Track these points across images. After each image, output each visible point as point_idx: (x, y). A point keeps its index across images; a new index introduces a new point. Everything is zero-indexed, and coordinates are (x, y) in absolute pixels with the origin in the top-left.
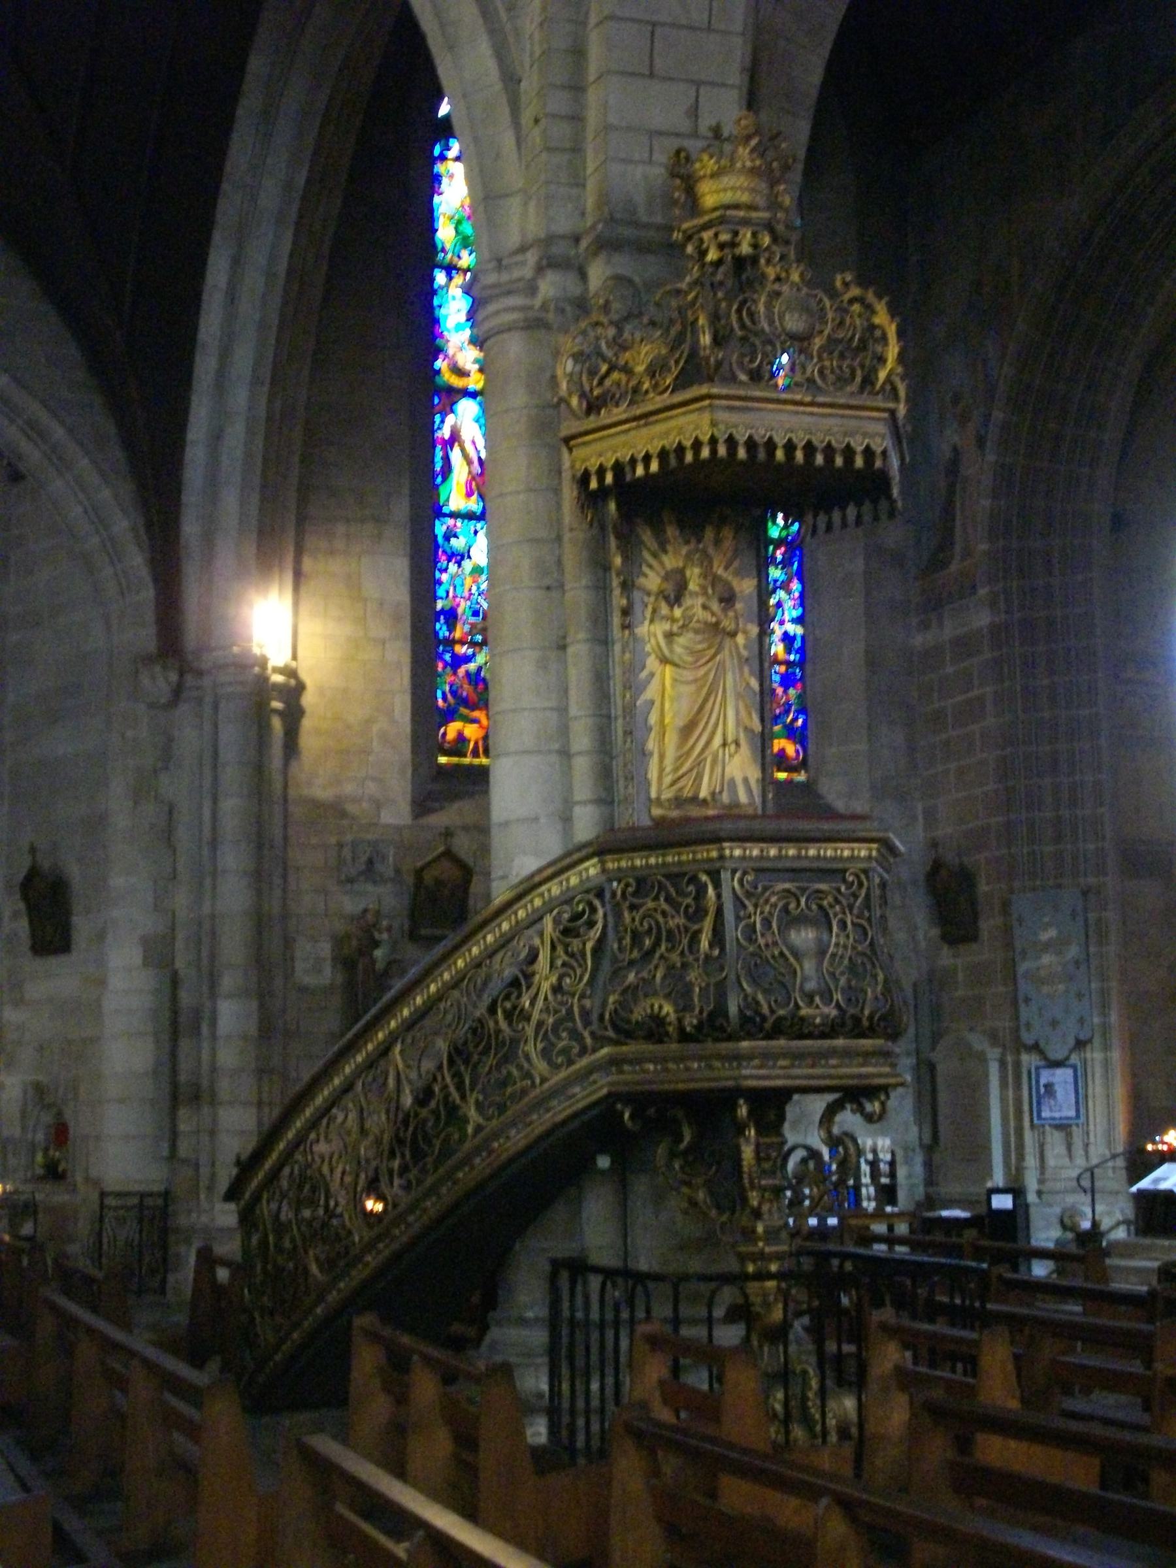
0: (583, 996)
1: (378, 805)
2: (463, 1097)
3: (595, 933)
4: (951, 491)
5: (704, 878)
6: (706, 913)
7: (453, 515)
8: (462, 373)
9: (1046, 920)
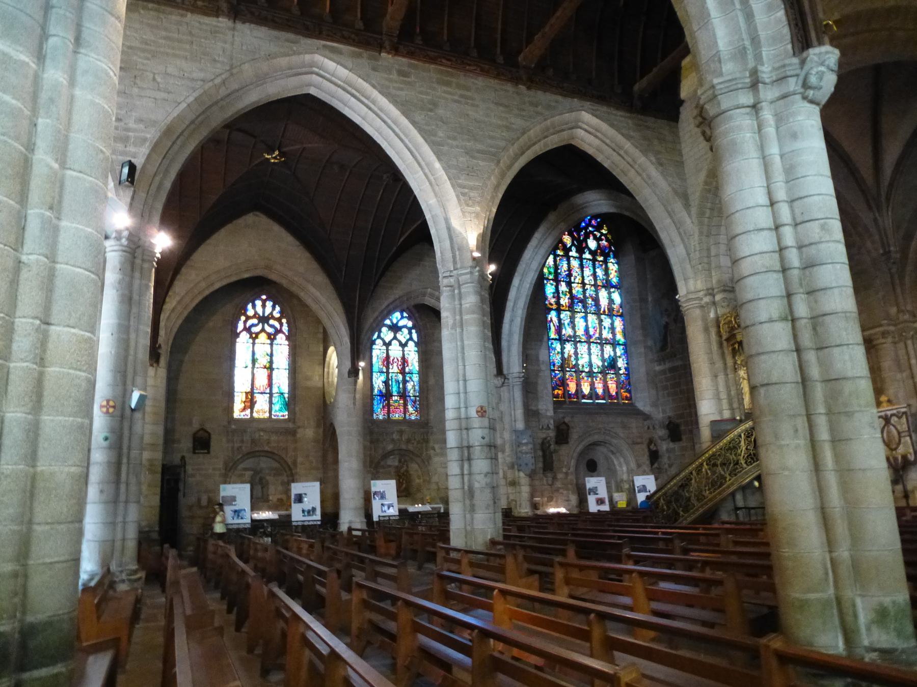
1: (546, 410)
7: (553, 339)
8: (551, 304)
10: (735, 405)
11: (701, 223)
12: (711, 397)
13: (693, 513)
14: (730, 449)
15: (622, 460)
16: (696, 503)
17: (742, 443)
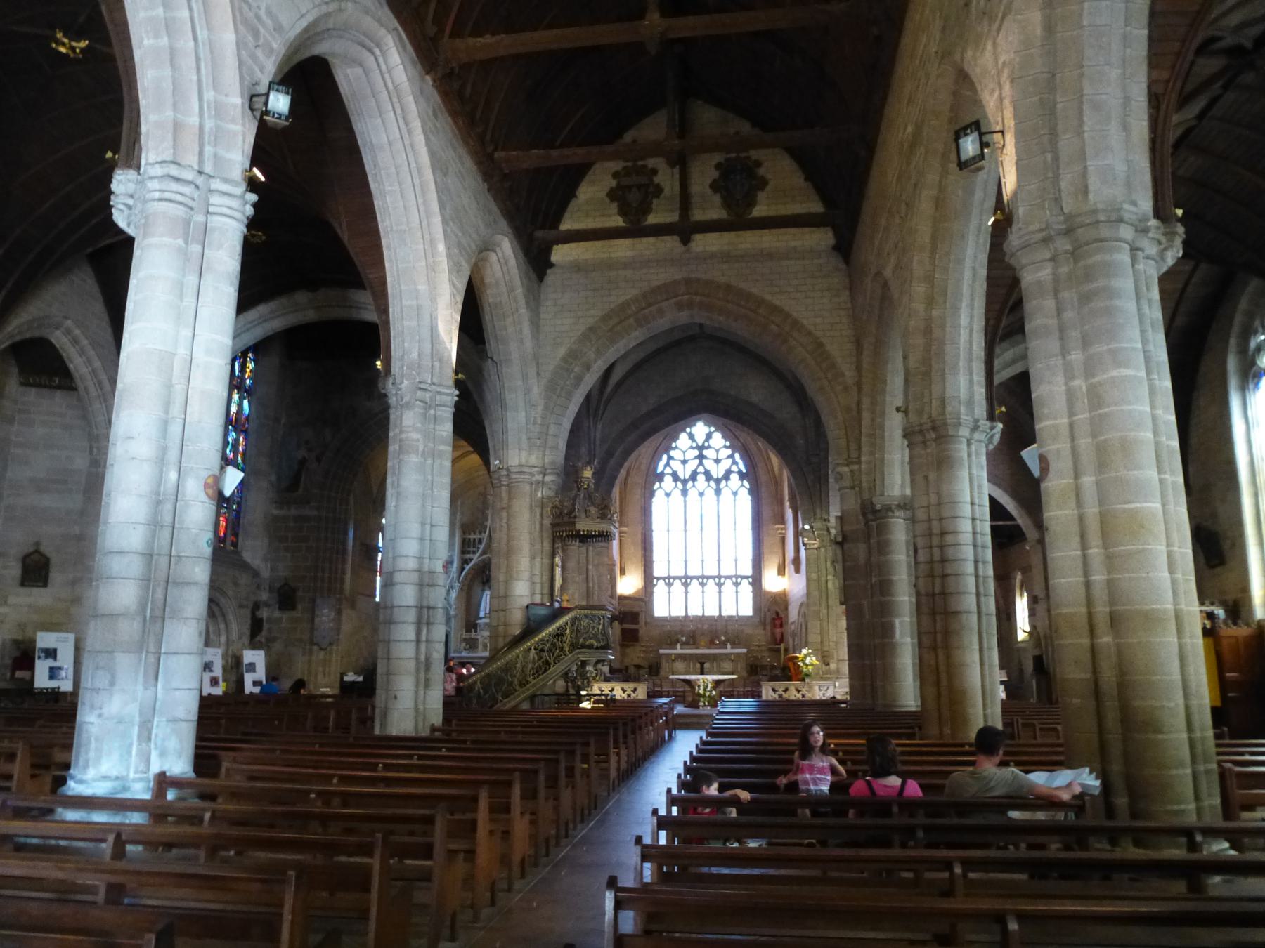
12: (527, 578)
13: (515, 698)
14: (557, 635)
15: (222, 626)
16: (517, 688)
17: (568, 631)
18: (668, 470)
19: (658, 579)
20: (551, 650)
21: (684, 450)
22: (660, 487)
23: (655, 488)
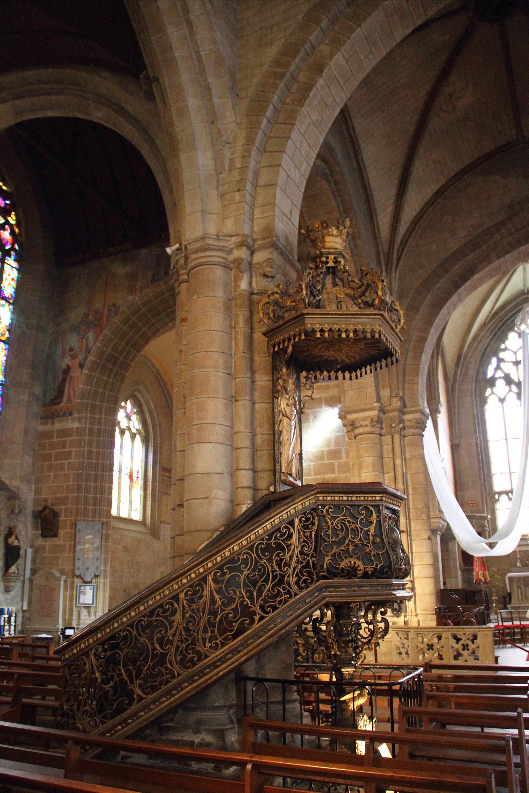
0: (312, 556)
2: (252, 602)
3: (315, 528)
4: (64, 380)
5: (371, 508)
6: (372, 523)
9: (89, 532)
10: (263, 463)
11: (253, 126)
12: (220, 439)
13: (168, 693)
16: (176, 669)
17: (294, 539)
18: (499, 374)
19: (500, 493)
20: (254, 583)
21: (515, 350)
22: (493, 393)
23: (487, 394)
